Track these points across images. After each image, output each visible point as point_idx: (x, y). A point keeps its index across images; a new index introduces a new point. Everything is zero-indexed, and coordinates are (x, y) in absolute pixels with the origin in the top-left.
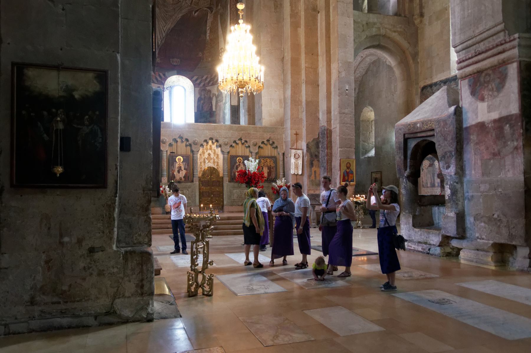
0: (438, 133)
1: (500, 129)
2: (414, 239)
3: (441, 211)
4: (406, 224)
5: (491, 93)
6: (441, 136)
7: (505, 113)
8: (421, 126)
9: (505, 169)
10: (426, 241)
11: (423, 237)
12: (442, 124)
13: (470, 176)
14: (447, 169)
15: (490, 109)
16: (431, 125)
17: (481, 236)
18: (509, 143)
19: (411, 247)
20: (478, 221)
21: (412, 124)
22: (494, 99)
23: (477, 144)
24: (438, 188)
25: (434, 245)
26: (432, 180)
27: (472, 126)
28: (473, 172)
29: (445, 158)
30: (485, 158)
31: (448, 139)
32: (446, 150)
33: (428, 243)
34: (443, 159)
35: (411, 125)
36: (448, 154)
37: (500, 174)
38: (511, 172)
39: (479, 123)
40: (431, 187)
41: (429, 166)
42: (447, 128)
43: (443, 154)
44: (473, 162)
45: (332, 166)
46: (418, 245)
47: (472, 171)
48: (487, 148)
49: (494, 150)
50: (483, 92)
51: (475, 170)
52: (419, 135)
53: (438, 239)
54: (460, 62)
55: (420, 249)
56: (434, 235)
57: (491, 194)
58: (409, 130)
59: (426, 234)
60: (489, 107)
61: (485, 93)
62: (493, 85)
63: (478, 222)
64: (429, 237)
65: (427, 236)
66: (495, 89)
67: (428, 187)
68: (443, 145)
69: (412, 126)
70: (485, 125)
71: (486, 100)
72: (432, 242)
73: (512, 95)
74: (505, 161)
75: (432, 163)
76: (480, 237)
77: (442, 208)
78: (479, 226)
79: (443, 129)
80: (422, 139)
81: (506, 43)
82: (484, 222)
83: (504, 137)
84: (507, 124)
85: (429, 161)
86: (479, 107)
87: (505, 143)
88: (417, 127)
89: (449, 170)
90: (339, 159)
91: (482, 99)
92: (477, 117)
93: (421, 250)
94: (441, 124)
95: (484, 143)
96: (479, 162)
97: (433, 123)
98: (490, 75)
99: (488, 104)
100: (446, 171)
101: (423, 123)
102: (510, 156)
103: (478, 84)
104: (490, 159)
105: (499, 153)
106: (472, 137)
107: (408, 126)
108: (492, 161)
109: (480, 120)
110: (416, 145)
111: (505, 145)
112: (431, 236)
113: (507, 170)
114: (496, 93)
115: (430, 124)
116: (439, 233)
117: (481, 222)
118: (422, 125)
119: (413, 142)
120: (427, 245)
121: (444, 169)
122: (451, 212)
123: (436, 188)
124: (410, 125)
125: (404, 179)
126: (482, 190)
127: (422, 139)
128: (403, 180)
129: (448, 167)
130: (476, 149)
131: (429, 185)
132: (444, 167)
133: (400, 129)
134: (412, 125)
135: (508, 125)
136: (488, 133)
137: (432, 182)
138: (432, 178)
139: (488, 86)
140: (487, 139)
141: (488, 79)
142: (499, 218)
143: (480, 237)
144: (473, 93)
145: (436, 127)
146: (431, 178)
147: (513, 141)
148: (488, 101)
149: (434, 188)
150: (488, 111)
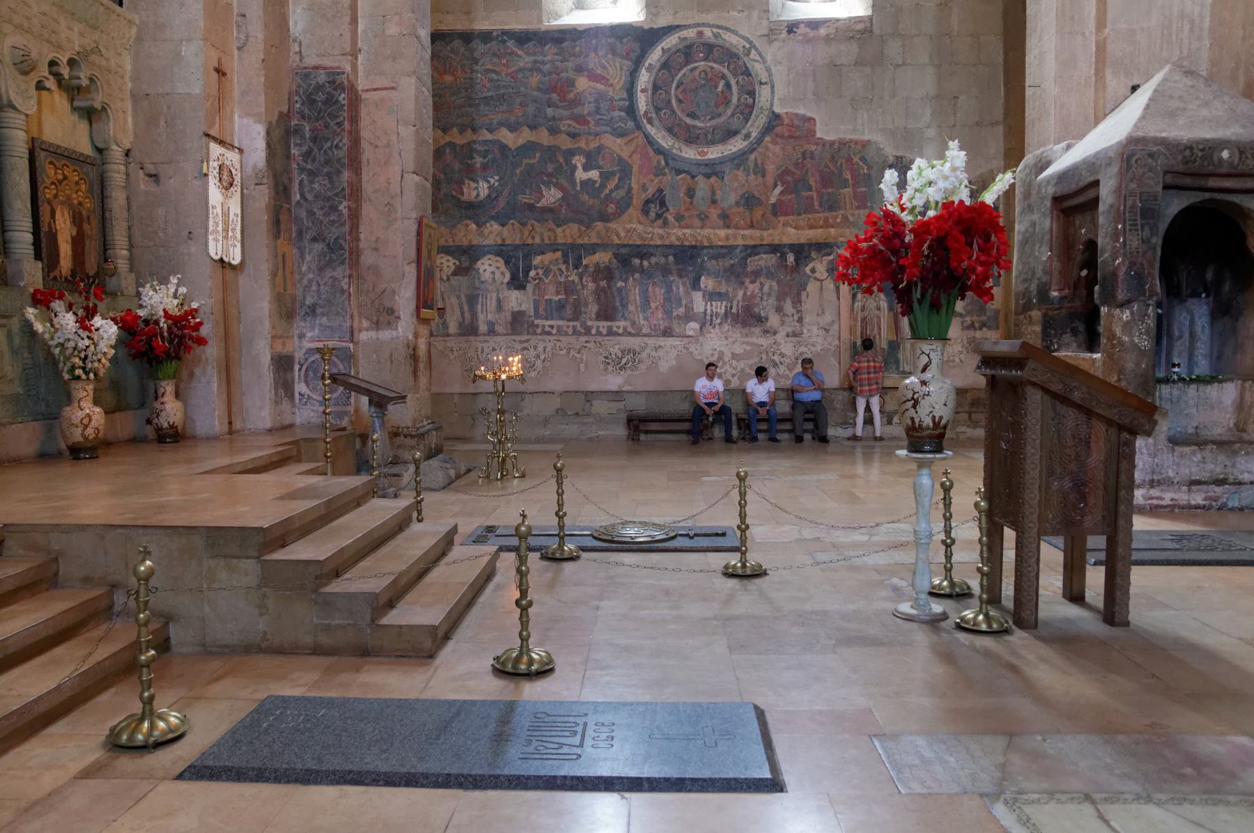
2: (1171, 474)
3: (1164, 395)
8: (1236, 161)
10: (1222, 476)
19: (1161, 499)
21: (1201, 147)
24: (487, 338)
26: (467, 315)
33: (1231, 479)
35: (1196, 151)
40: (462, 335)
41: (454, 274)
45: (358, 240)
46: (1189, 490)
52: (1213, 183)
55: (1198, 499)
64: (1234, 466)
65: (1228, 463)
67: (448, 335)
69: (1200, 154)
75: (465, 264)
77: (1168, 386)
80: (1207, 195)
85: (454, 258)
88: (1221, 159)
90: (414, 215)
93: (1204, 503)
107: (1181, 152)
118: (1237, 155)
119: (1176, 201)
120: (1227, 486)
123: (481, 338)
124: (1191, 148)
125: (1149, 305)
127: (1207, 195)
131: (453, 328)
133: (1151, 155)
134: (1202, 150)
137: (467, 322)
138: (466, 308)
146: (461, 308)
149: (472, 338)
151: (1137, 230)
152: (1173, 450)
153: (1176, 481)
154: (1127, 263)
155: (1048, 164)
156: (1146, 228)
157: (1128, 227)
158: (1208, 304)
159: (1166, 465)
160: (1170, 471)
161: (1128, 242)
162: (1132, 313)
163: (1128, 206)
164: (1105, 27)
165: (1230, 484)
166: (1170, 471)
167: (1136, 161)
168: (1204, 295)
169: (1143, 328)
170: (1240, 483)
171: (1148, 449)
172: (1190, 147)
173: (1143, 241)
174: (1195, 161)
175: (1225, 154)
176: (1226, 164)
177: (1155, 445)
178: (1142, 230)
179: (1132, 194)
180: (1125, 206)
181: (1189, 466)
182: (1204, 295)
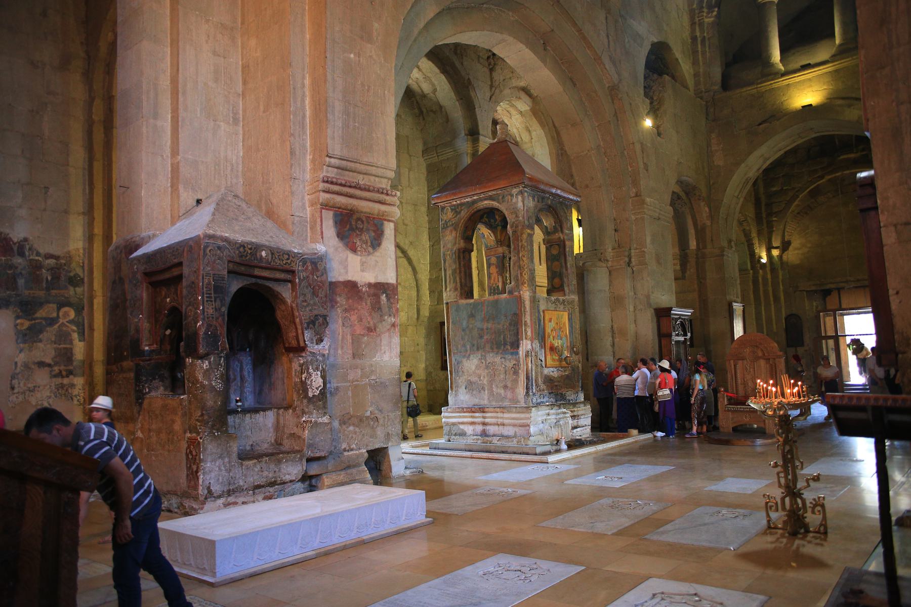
0: (303, 280)
1: (377, 296)
2: (241, 483)
4: (221, 457)
5: (364, 246)
6: (307, 287)
7: (381, 279)
9: (381, 350)
10: (273, 479)
11: (265, 473)
12: (310, 268)
13: (335, 356)
14: (317, 344)
15: (364, 267)
16: (289, 261)
17: (349, 447)
18: (386, 317)
20: (344, 424)
21: (250, 246)
22: (368, 255)
23: (346, 310)
25: (291, 481)
27: (340, 282)
28: (340, 352)
29: (314, 325)
30: (358, 332)
31: (320, 295)
32: (316, 312)
34: (311, 326)
36: (321, 320)
37: (375, 356)
38: (388, 354)
39: (349, 281)
42: (317, 277)
43: (312, 318)
44: (340, 337)
47: (337, 351)
48: (361, 320)
49: (369, 323)
50: (355, 241)
51: (342, 348)
52: (257, 272)
53: (300, 468)
54: (327, 182)
56: (290, 463)
57: (363, 383)
58: (241, 256)
59: (272, 466)
60: (363, 264)
61: (358, 243)
62: (366, 237)
63: (344, 427)
64: (280, 471)
66: (369, 244)
68: (311, 302)
70: (358, 287)
71: (359, 253)
72: (287, 478)
73: (389, 259)
74: (381, 340)
76: (347, 448)
77: (232, 416)
78: (346, 432)
79: (311, 276)
80: (254, 280)
81: (387, 194)
82: (354, 425)
83: (380, 309)
84: (383, 293)
86: (349, 259)
87: (381, 316)
89: (320, 347)
91: (354, 250)
92: (347, 273)
94: (307, 266)
95: (356, 311)
96: (349, 337)
97: (293, 260)
98: (363, 222)
99: (361, 260)
100: (316, 347)
101: (272, 254)
102: (387, 334)
103: (348, 226)
104: (363, 335)
105: (375, 330)
106: (338, 299)
107: (238, 248)
108: (366, 338)
109: (350, 277)
110: (240, 291)
111: (382, 320)
112: (283, 466)
113: (383, 352)
114: (370, 249)
115: (288, 259)
116: (301, 456)
117: (350, 425)
120: (276, 487)
121: (312, 343)
122: (324, 416)
125: (221, 357)
126: (351, 378)
127: (254, 280)
128: (220, 360)
129: (320, 341)
130: (345, 317)
132: (312, 339)
133: (219, 248)
134: (251, 249)
135: (384, 295)
136: (361, 298)
139: (361, 235)
140: (360, 307)
141: (361, 227)
142: (372, 416)
143: (347, 448)
144: (341, 236)
145: (300, 268)
147: (390, 315)
148: (361, 256)
150: (361, 270)
151: (212, 301)
152: (242, 465)
153: (245, 488)
154: (205, 325)
155: (137, 247)
156: (218, 300)
157: (205, 299)
158: (250, 356)
159: (237, 477)
160: (241, 481)
161: (206, 310)
162: (210, 363)
163: (205, 283)
164: (178, 154)
165: (278, 484)
166: (241, 481)
167: (210, 251)
168: (248, 350)
169: (218, 374)
170: (284, 483)
171: (225, 467)
172: (243, 245)
173: (216, 310)
174: (247, 256)
175: (264, 254)
176: (264, 260)
177: (230, 462)
178: (215, 301)
179: (208, 274)
180: (203, 283)
181: (252, 475)
182: (248, 350)
